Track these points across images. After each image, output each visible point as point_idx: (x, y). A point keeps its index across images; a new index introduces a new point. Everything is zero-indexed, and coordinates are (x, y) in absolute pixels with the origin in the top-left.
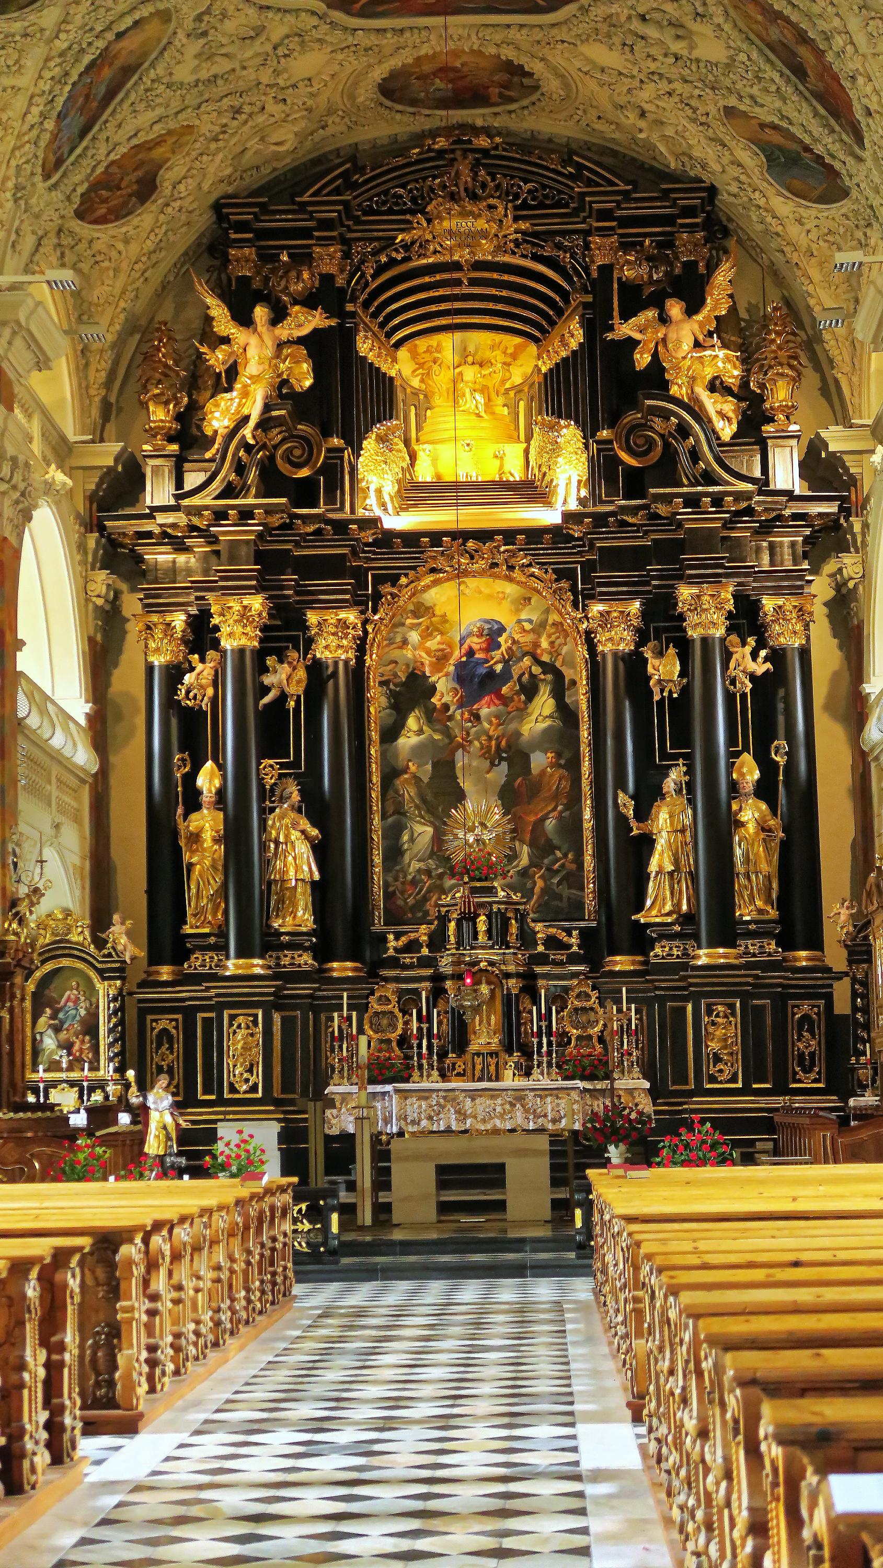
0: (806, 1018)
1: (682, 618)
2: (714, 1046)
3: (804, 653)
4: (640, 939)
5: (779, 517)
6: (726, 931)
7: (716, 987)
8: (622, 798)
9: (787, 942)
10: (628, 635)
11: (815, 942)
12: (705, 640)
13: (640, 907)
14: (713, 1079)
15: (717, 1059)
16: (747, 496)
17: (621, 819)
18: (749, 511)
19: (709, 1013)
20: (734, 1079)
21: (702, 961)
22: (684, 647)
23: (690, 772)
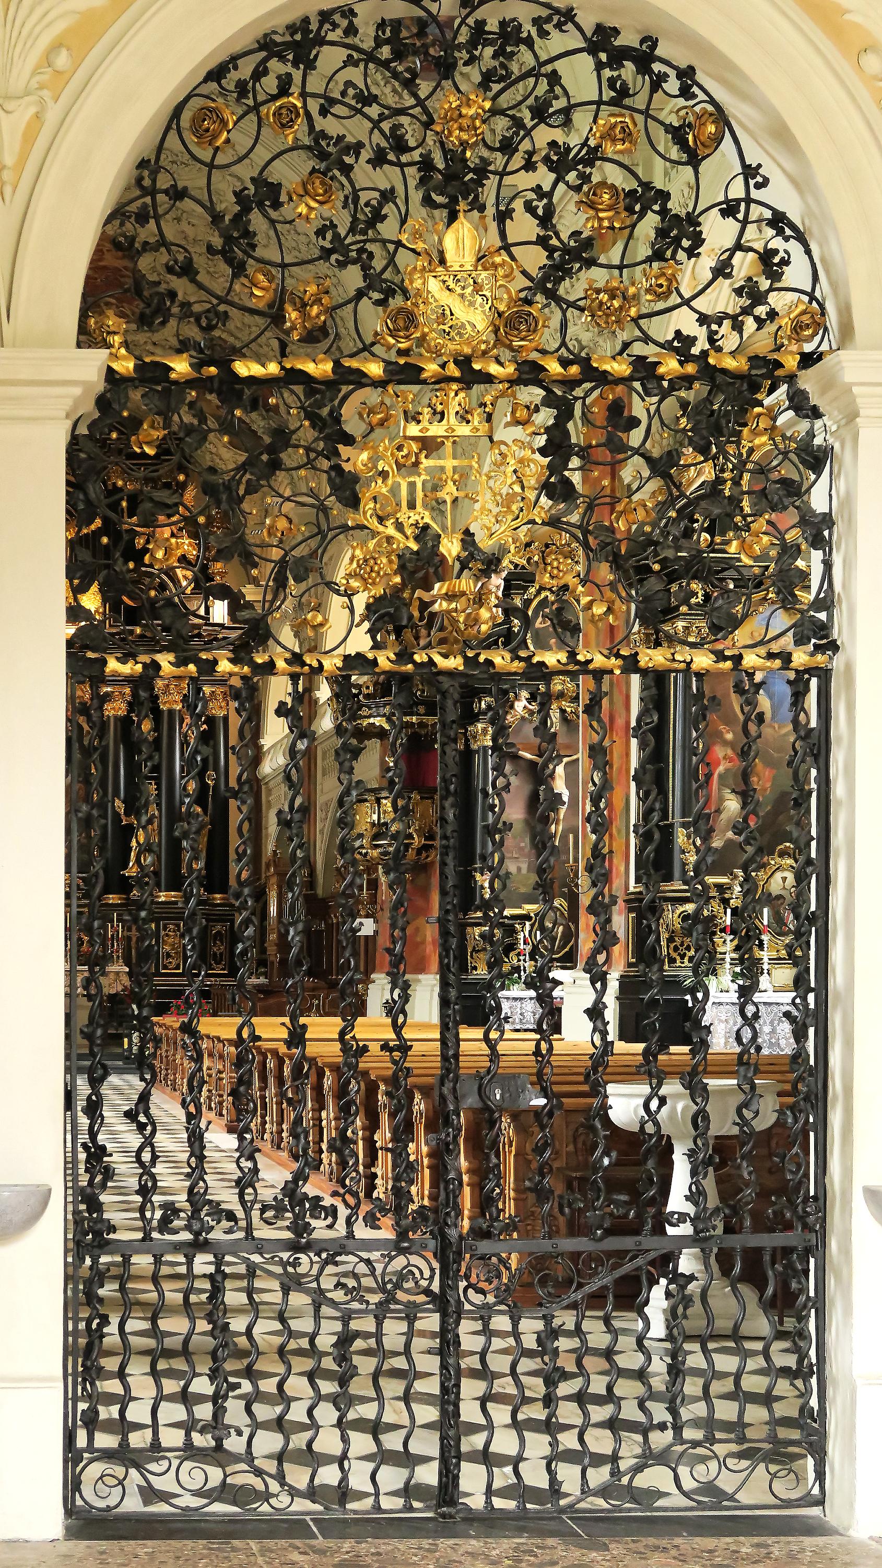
0: (219, 933)
1: (157, 697)
2: (167, 948)
3: (226, 719)
4: (124, 885)
5: (216, 639)
6: (175, 883)
7: (168, 913)
8: (118, 803)
9: (210, 890)
10: (124, 706)
11: (224, 889)
12: (171, 712)
13: (125, 866)
14: (165, 967)
15: (168, 955)
16: (198, 627)
17: (116, 815)
18: (199, 635)
19: (165, 929)
20: (178, 968)
21: (162, 899)
22: (157, 713)
23: (158, 785)
